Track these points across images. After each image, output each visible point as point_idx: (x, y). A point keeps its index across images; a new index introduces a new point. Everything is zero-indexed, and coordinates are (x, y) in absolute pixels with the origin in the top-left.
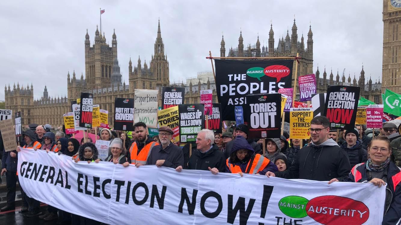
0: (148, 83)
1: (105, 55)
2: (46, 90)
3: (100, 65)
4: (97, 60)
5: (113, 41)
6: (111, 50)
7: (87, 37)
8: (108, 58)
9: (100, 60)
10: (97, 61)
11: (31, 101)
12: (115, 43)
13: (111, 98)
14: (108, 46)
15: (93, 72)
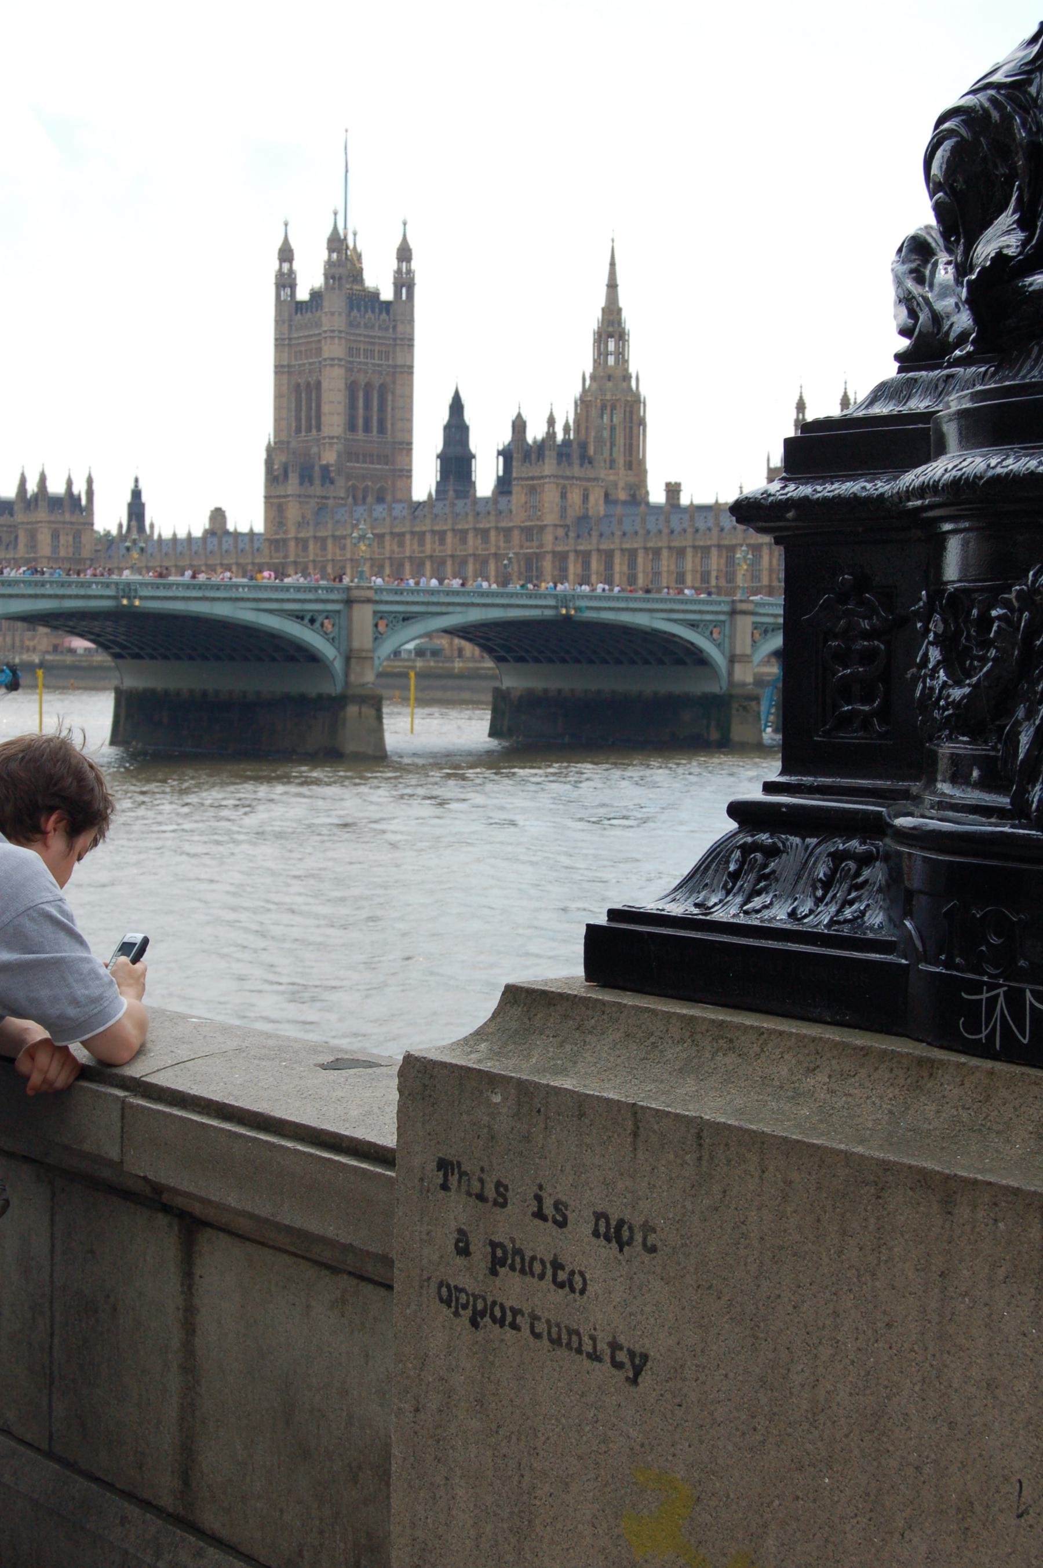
0: (578, 491)
1: (362, 339)
2: (136, 494)
3: (341, 384)
4: (332, 359)
5: (399, 271)
6: (388, 313)
7: (286, 254)
8: (377, 348)
9: (343, 363)
10: (332, 366)
11: (85, 539)
12: (404, 282)
13: (442, 541)
14: (376, 295)
15: (309, 409)
